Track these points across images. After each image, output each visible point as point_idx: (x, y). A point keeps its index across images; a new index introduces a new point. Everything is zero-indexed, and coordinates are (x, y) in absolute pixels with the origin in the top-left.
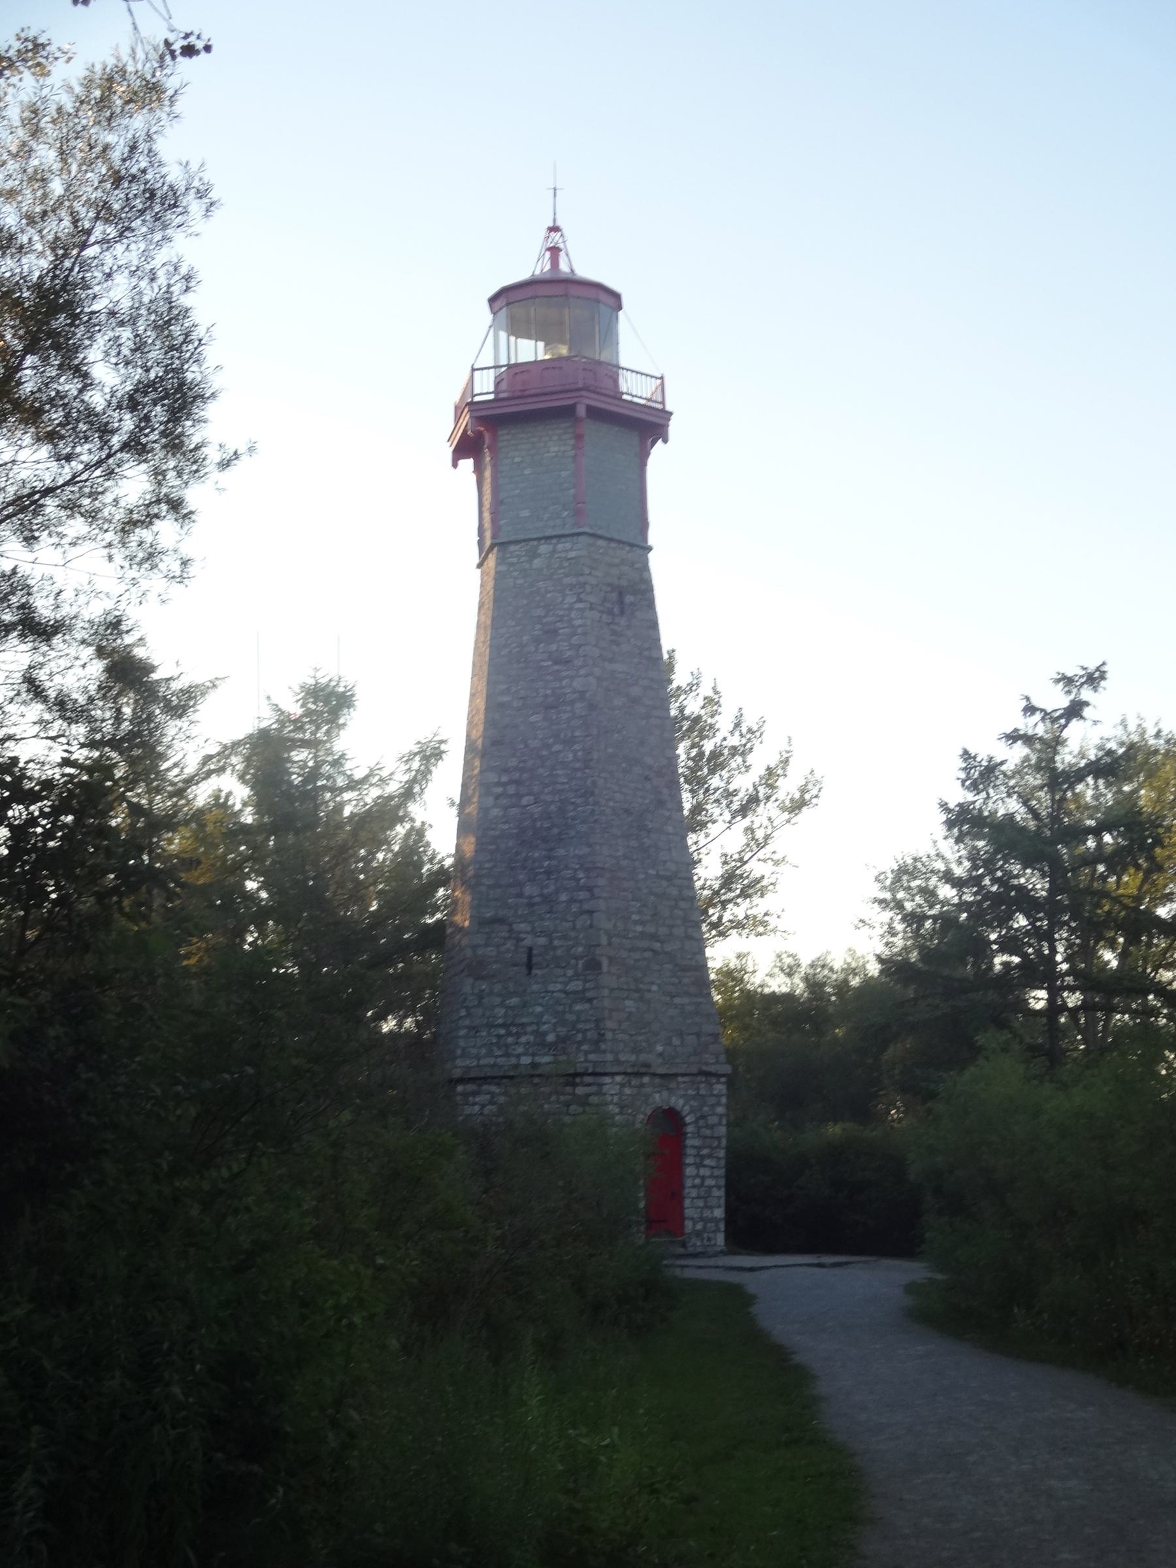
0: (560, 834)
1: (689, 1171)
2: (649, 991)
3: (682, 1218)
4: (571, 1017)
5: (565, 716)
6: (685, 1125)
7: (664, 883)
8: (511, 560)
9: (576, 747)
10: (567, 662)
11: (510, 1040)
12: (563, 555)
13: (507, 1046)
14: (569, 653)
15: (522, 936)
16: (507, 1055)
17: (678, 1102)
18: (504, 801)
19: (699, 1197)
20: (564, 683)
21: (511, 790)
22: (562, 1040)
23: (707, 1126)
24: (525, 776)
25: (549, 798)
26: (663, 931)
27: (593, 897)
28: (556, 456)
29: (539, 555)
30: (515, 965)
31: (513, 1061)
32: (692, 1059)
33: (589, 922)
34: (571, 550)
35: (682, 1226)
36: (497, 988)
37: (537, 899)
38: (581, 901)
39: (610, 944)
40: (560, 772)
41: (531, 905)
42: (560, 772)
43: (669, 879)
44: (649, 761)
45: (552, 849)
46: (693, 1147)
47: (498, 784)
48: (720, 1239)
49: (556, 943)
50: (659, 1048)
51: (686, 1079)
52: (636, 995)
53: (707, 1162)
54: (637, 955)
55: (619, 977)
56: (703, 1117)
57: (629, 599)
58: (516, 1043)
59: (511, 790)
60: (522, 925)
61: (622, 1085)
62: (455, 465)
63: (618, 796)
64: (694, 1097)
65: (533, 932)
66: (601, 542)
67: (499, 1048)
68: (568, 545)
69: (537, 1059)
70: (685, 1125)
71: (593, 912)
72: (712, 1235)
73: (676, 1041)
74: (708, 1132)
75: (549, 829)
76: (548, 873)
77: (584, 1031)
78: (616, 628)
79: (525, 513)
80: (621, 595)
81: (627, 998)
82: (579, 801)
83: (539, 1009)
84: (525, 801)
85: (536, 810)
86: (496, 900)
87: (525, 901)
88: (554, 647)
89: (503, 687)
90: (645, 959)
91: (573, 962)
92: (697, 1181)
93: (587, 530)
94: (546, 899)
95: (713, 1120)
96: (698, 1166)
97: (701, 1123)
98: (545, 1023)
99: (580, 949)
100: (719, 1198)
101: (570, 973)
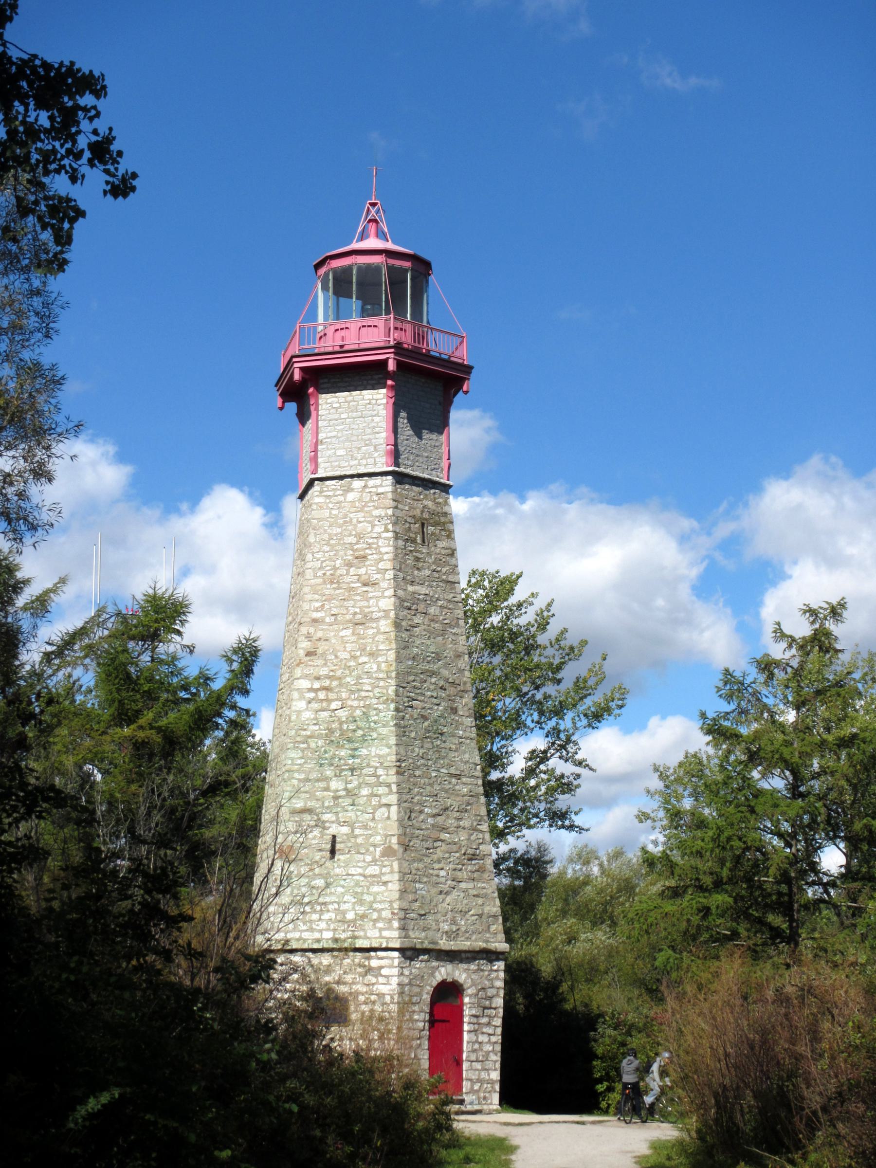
0: (364, 735)
2: (438, 876)
4: (368, 898)
5: (371, 632)
7: (454, 780)
8: (330, 493)
9: (380, 659)
11: (315, 917)
12: (374, 490)
13: (311, 921)
14: (376, 576)
16: (311, 930)
18: (315, 706)
20: (371, 602)
24: (335, 683)
25: (355, 703)
28: (369, 404)
30: (320, 850)
31: (317, 935)
33: (386, 815)
34: (381, 486)
37: (343, 793)
38: (379, 796)
40: (364, 681)
41: (336, 798)
42: (364, 681)
43: (458, 777)
44: (445, 673)
45: (356, 749)
47: (311, 690)
48: (496, 1098)
49: (357, 832)
51: (469, 955)
58: (320, 919)
59: (322, 695)
60: (329, 816)
67: (305, 924)
72: (487, 1095)
75: (354, 731)
77: (379, 911)
79: (341, 452)
80: (423, 525)
82: (381, 707)
83: (340, 890)
84: (334, 706)
85: (343, 714)
87: (332, 794)
88: (363, 571)
89: (317, 605)
91: (372, 849)
92: (476, 1046)
93: (397, 469)
95: (490, 992)
99: (379, 838)
100: (495, 1062)
101: (369, 858)
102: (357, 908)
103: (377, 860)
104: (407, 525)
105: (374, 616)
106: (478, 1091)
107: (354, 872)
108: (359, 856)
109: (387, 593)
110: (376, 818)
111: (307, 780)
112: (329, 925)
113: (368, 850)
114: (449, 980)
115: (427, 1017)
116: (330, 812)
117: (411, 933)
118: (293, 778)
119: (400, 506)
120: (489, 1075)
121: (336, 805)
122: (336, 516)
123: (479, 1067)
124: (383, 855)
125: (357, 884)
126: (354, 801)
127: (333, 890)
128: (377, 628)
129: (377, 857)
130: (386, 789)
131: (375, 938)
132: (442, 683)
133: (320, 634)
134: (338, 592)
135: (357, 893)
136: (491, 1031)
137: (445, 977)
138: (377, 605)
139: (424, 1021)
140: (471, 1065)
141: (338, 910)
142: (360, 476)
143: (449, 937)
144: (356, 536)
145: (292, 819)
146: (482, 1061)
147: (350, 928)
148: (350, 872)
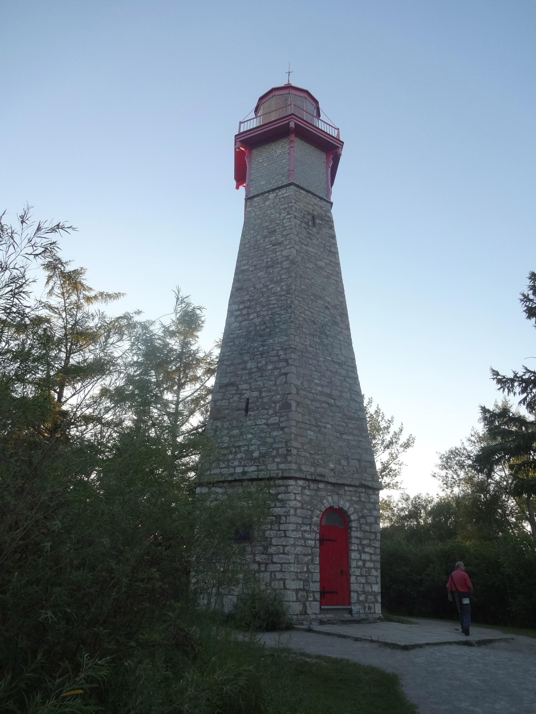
1: (354, 555)
2: (325, 427)
3: (349, 591)
4: (269, 440)
6: (351, 521)
7: (337, 366)
9: (282, 284)
10: (280, 244)
11: (231, 457)
13: (228, 461)
15: (244, 392)
16: (228, 467)
17: (346, 505)
18: (240, 319)
19: (361, 576)
20: (278, 254)
21: (244, 312)
22: (263, 455)
23: (367, 524)
25: (265, 313)
26: (335, 393)
27: (288, 364)
29: (269, 199)
30: (238, 410)
31: (232, 470)
32: (356, 476)
33: (284, 380)
34: (286, 193)
35: (349, 597)
36: (226, 425)
39: (298, 394)
41: (250, 374)
43: (340, 364)
45: (265, 341)
46: (357, 538)
47: (239, 310)
48: (378, 609)
50: (332, 466)
51: (351, 489)
52: (314, 428)
53: (367, 550)
54: (318, 405)
55: (303, 415)
56: (363, 517)
57: (318, 221)
60: (244, 385)
61: (303, 488)
62: (237, 188)
63: (308, 313)
64: (357, 502)
65: (251, 390)
66: (302, 191)
67: (223, 462)
68: (284, 191)
69: (246, 469)
70: (351, 521)
71: (287, 373)
72: (372, 605)
73: (343, 462)
74: (367, 528)
75: (264, 329)
76: (262, 354)
77: (278, 449)
78: (310, 232)
81: (309, 429)
82: (282, 312)
83: (250, 436)
85: (257, 321)
86: (231, 373)
88: (274, 238)
89: (244, 262)
90: (323, 408)
91: (273, 405)
92: (360, 563)
94: (259, 369)
96: (361, 552)
97: (362, 521)
98: (252, 445)
99: (278, 397)
100: (376, 577)
101: (271, 412)
102: (261, 449)
103: (277, 413)
104: (302, 214)
105: (279, 261)
106: (362, 601)
107: (260, 423)
108: (264, 411)
109: (288, 247)
110: (278, 383)
111: (232, 364)
112: (241, 463)
113: (270, 406)
114: (336, 507)
115: (318, 537)
116: (246, 383)
117: (303, 468)
118: (223, 365)
119: (297, 203)
120: (371, 588)
121: (251, 378)
122: (259, 215)
123: (363, 581)
124: (281, 408)
125: (262, 431)
126: (262, 374)
127: (245, 437)
128: (282, 267)
129: (277, 410)
130: (285, 363)
131: (274, 470)
132: (327, 305)
133: (246, 277)
134: (257, 253)
135: (261, 437)
136: (372, 551)
137: (332, 505)
138: (281, 254)
139: (315, 540)
140: (357, 579)
141: (248, 450)
142: (273, 190)
143: (334, 473)
144: (269, 221)
145: (220, 391)
146: (366, 576)
147: (256, 464)
148: (257, 423)
